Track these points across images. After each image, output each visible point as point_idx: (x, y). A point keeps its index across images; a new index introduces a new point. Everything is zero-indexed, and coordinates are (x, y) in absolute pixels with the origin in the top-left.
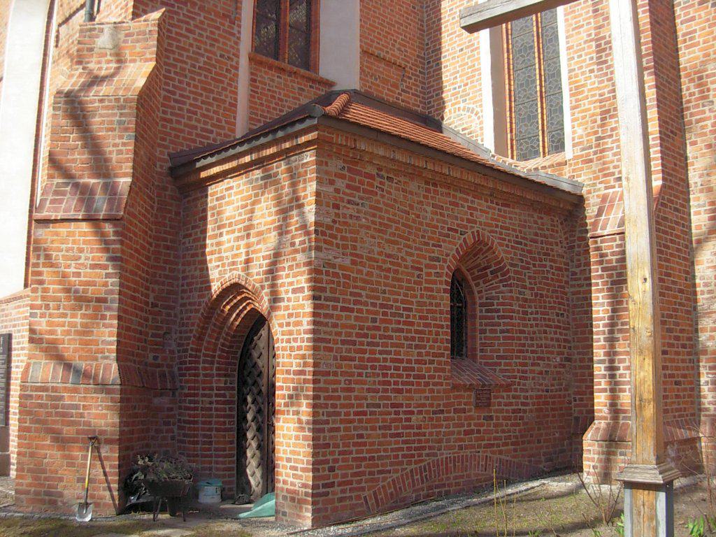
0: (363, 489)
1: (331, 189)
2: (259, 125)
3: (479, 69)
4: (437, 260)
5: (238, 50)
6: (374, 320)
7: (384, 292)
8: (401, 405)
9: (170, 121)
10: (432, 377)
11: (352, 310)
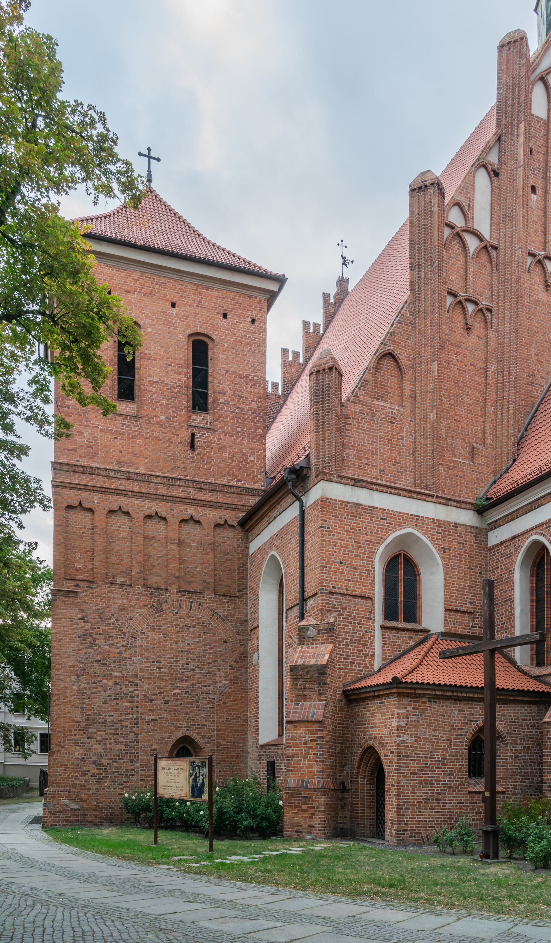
0: (421, 833)
1: (404, 711)
5: (374, 627)
6: (426, 764)
7: (431, 752)
8: (440, 800)
9: (342, 669)
11: (415, 760)
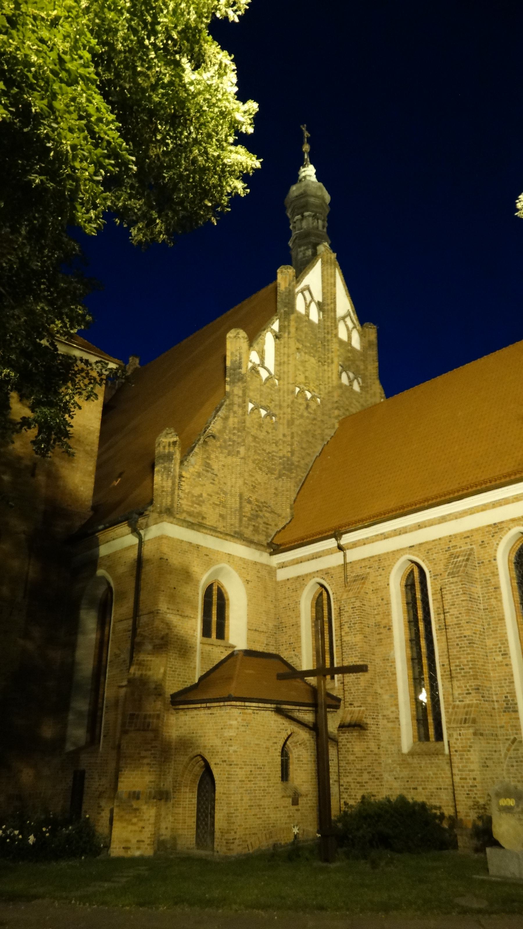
2: (204, 673)
3: (300, 637)
4: (276, 743)
6: (251, 771)
8: (261, 805)
10: (274, 793)
11: (242, 768)
